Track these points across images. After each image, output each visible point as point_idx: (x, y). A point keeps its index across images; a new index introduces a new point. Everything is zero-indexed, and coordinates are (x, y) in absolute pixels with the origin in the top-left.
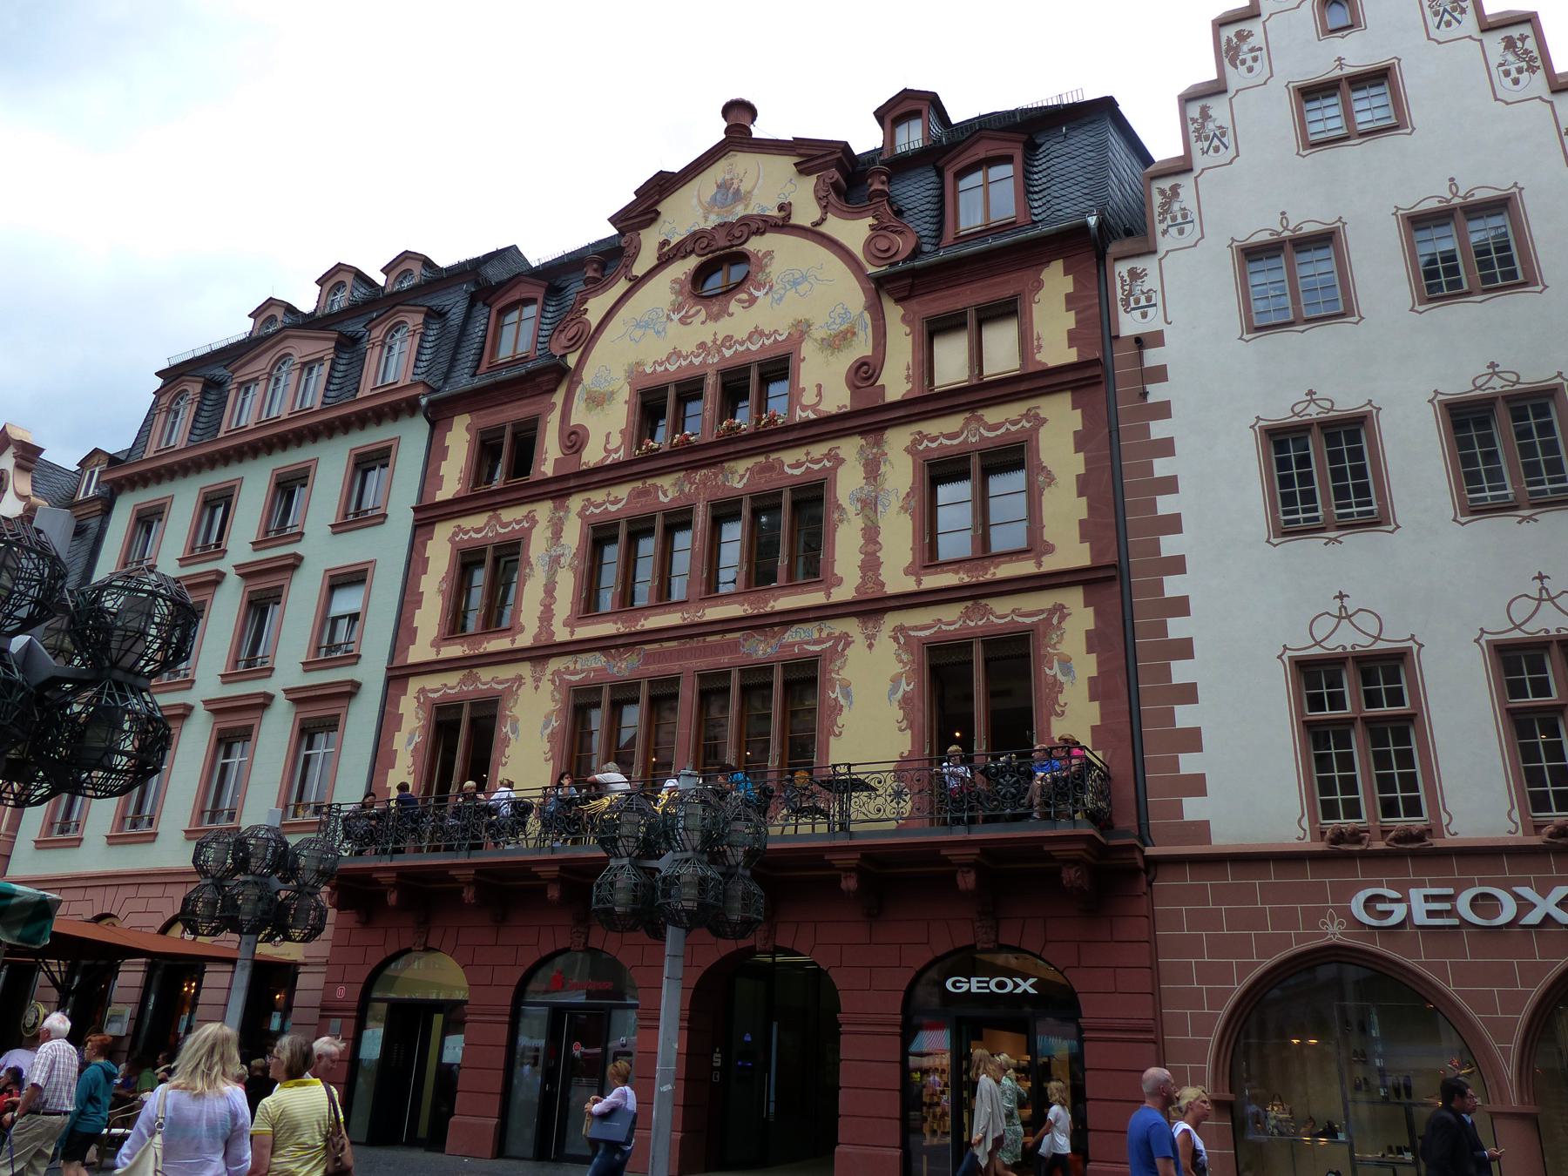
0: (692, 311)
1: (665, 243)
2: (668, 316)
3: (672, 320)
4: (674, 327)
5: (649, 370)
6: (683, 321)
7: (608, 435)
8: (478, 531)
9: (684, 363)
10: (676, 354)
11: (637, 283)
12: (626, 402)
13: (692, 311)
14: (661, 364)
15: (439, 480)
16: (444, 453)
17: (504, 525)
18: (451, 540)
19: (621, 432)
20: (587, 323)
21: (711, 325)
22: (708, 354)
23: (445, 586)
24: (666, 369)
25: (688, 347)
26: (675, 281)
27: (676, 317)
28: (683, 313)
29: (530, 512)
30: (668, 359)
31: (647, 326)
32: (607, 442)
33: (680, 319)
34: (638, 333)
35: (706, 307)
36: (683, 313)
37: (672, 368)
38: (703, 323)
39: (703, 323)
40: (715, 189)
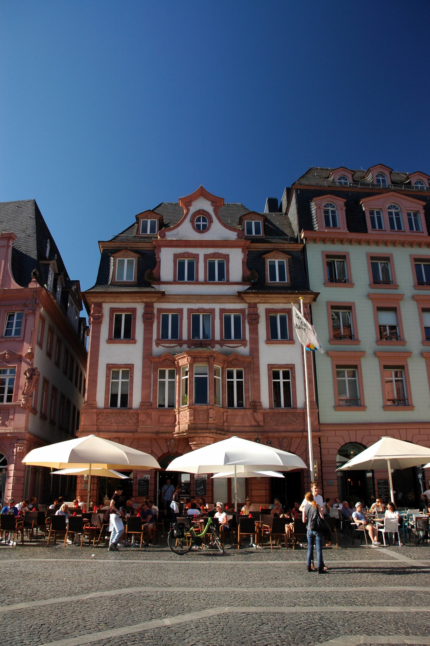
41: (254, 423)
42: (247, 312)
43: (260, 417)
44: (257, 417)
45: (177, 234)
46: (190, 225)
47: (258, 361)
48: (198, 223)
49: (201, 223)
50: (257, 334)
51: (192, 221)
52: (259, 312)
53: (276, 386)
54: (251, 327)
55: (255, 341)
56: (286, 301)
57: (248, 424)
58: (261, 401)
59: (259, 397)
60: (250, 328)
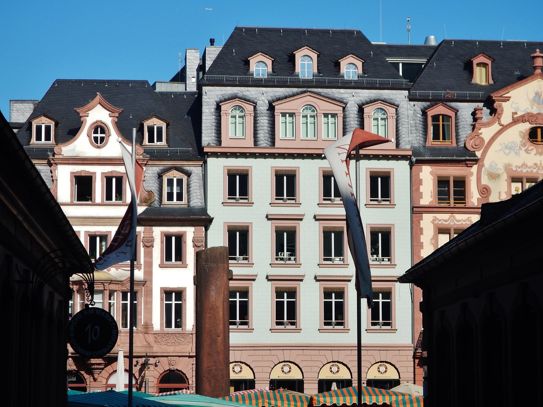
0: (530, 148)
1: (516, 113)
2: (520, 147)
3: (521, 149)
4: (523, 153)
5: (515, 169)
6: (527, 151)
7: (500, 193)
8: (446, 221)
9: (529, 170)
10: (524, 165)
11: (504, 128)
12: (506, 180)
13: (530, 148)
14: (519, 168)
15: (421, 196)
16: (420, 182)
17: (458, 221)
18: (433, 222)
19: (505, 192)
20: (483, 140)
21: (538, 156)
22: (539, 169)
23: (434, 241)
24: (522, 171)
25: (530, 163)
26: (521, 132)
27: (523, 149)
28: (526, 148)
29: (468, 218)
30: (522, 166)
31: (510, 148)
32: (500, 196)
33: (525, 150)
34: (507, 151)
35: (536, 148)
36: (526, 148)
37: (525, 171)
38: (535, 155)
39: (535, 155)
40: (534, 95)
41: (145, 343)
42: (142, 235)
43: (151, 338)
44: (148, 338)
45: (74, 150)
46: (87, 139)
47: (151, 284)
48: (96, 135)
49: (99, 135)
50: (151, 257)
51: (89, 136)
52: (154, 234)
53: (168, 307)
54: (146, 250)
55: (149, 265)
56: (182, 224)
57: (139, 346)
58: (153, 323)
59: (151, 319)
60: (144, 251)
